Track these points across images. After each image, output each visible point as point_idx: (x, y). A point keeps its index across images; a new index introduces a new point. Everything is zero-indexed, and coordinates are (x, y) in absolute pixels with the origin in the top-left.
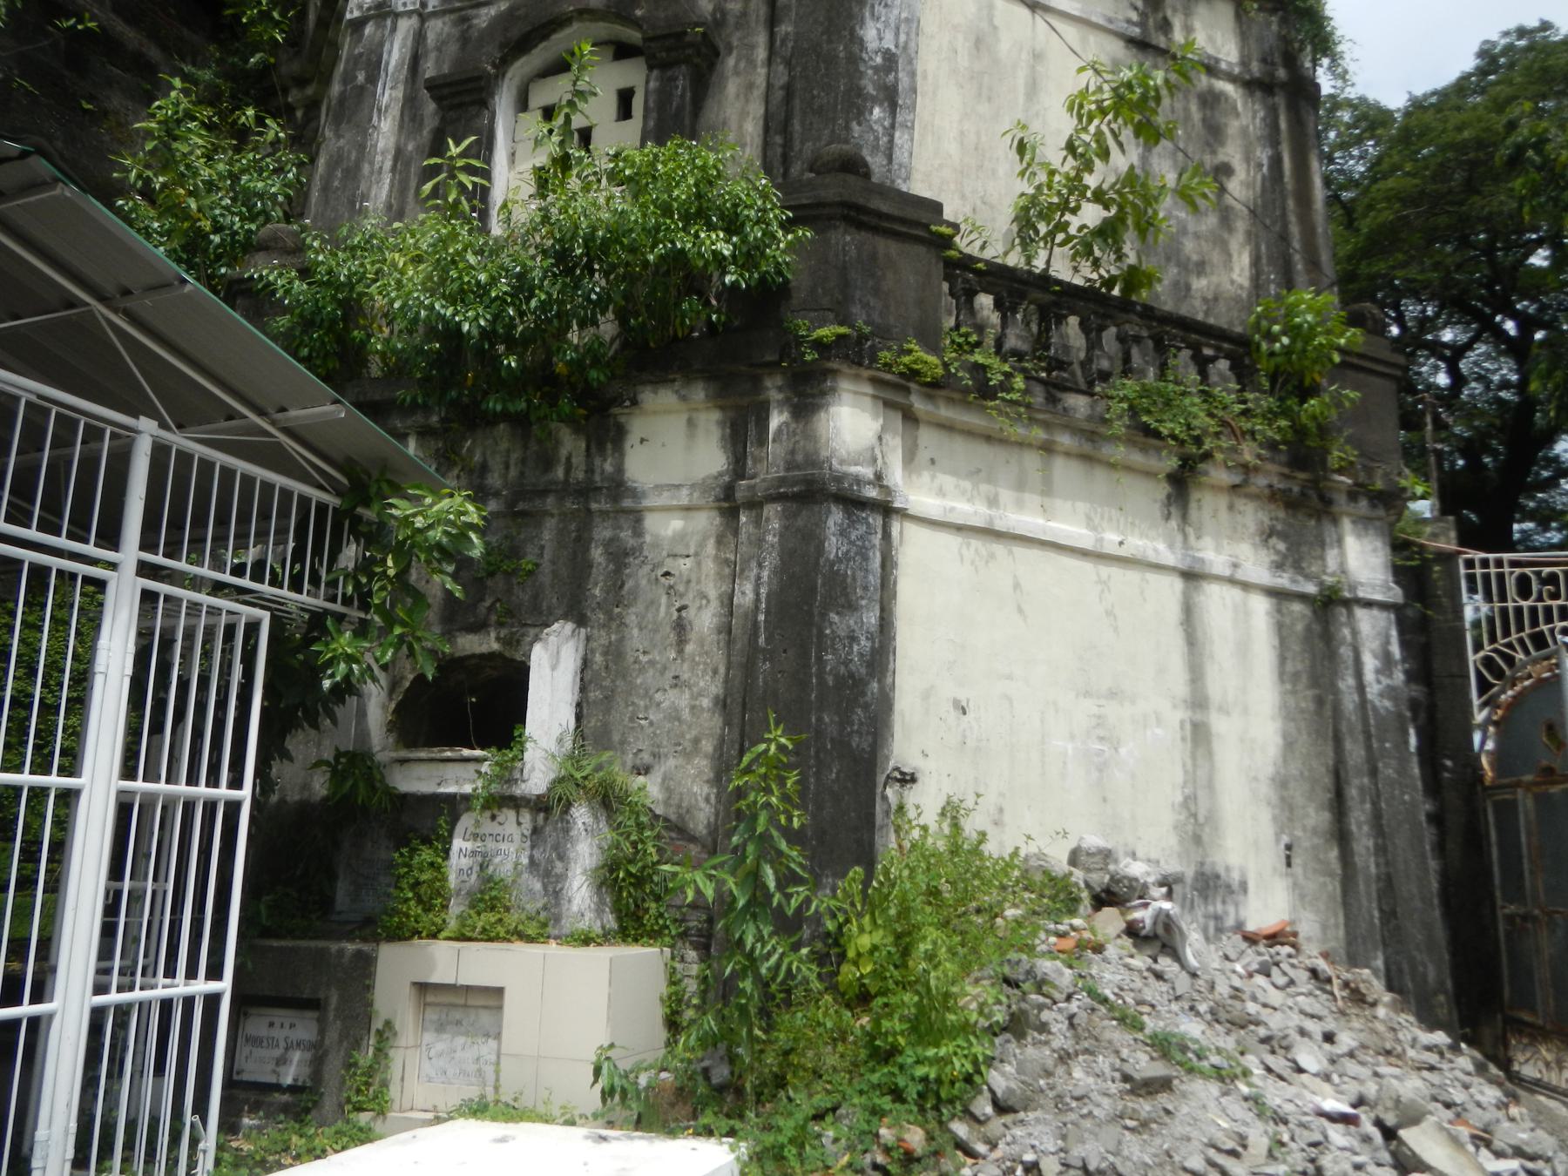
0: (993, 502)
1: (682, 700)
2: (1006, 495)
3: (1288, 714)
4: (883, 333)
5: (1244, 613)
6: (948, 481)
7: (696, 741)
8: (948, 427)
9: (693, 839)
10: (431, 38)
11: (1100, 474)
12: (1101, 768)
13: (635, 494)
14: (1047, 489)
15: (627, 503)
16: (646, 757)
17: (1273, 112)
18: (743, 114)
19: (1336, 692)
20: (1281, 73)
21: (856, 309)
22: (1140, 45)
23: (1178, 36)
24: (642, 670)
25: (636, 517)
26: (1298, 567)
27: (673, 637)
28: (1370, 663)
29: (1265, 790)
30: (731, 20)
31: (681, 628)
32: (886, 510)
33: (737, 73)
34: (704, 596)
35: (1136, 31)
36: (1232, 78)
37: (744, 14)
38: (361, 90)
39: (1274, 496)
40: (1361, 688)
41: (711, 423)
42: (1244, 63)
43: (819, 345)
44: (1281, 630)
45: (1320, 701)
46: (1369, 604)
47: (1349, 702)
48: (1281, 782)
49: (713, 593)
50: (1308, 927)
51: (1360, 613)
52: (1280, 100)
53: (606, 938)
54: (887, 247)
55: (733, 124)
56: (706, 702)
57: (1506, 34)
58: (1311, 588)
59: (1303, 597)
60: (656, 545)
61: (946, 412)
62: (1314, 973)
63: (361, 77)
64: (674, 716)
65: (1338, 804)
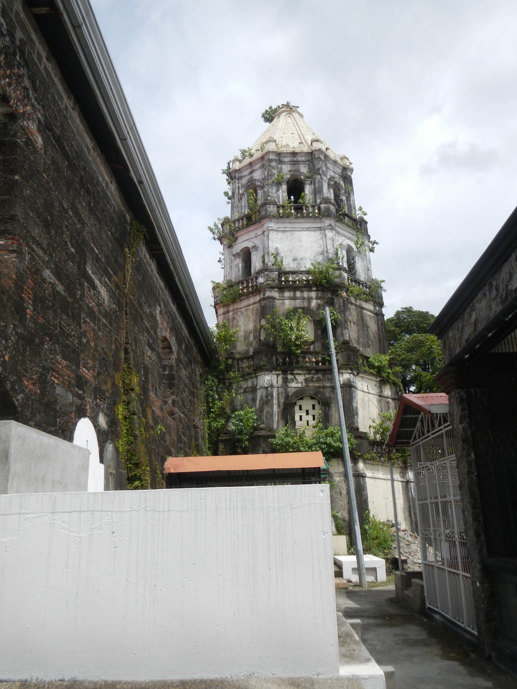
0: (373, 473)
1: (342, 503)
2: (374, 472)
3: (404, 499)
4: (364, 453)
5: (398, 485)
6: (369, 471)
7: (345, 508)
8: (368, 463)
9: (346, 521)
10: (280, 391)
11: (383, 467)
12: (386, 509)
13: (331, 474)
14: (378, 470)
15: (331, 475)
16: (338, 511)
17: (395, 403)
18: (336, 414)
19: (409, 495)
20: (397, 397)
21: (361, 451)
22: (380, 396)
23: (384, 393)
24: (336, 499)
25: (332, 477)
26: (404, 478)
27: (340, 494)
28: (413, 491)
29: (402, 510)
30: (332, 398)
31: (341, 493)
32: (365, 477)
33: (334, 407)
34: (343, 489)
35: (379, 394)
36: (390, 398)
37: (334, 397)
38: (270, 400)
39: (401, 467)
40: (412, 494)
41: (341, 463)
42: (392, 394)
43: (358, 456)
44: (402, 487)
45: (407, 497)
46: (412, 482)
47: (411, 496)
48: (404, 509)
49: (345, 488)
50: (407, 529)
51: (411, 483)
52: (396, 401)
53: (336, 535)
54: (363, 441)
55: (334, 415)
56: (346, 503)
57: (402, 308)
58: (405, 480)
59: (404, 482)
60: (335, 481)
61: (369, 462)
62: (410, 535)
63: (270, 398)
64: (341, 505)
65: (410, 512)
